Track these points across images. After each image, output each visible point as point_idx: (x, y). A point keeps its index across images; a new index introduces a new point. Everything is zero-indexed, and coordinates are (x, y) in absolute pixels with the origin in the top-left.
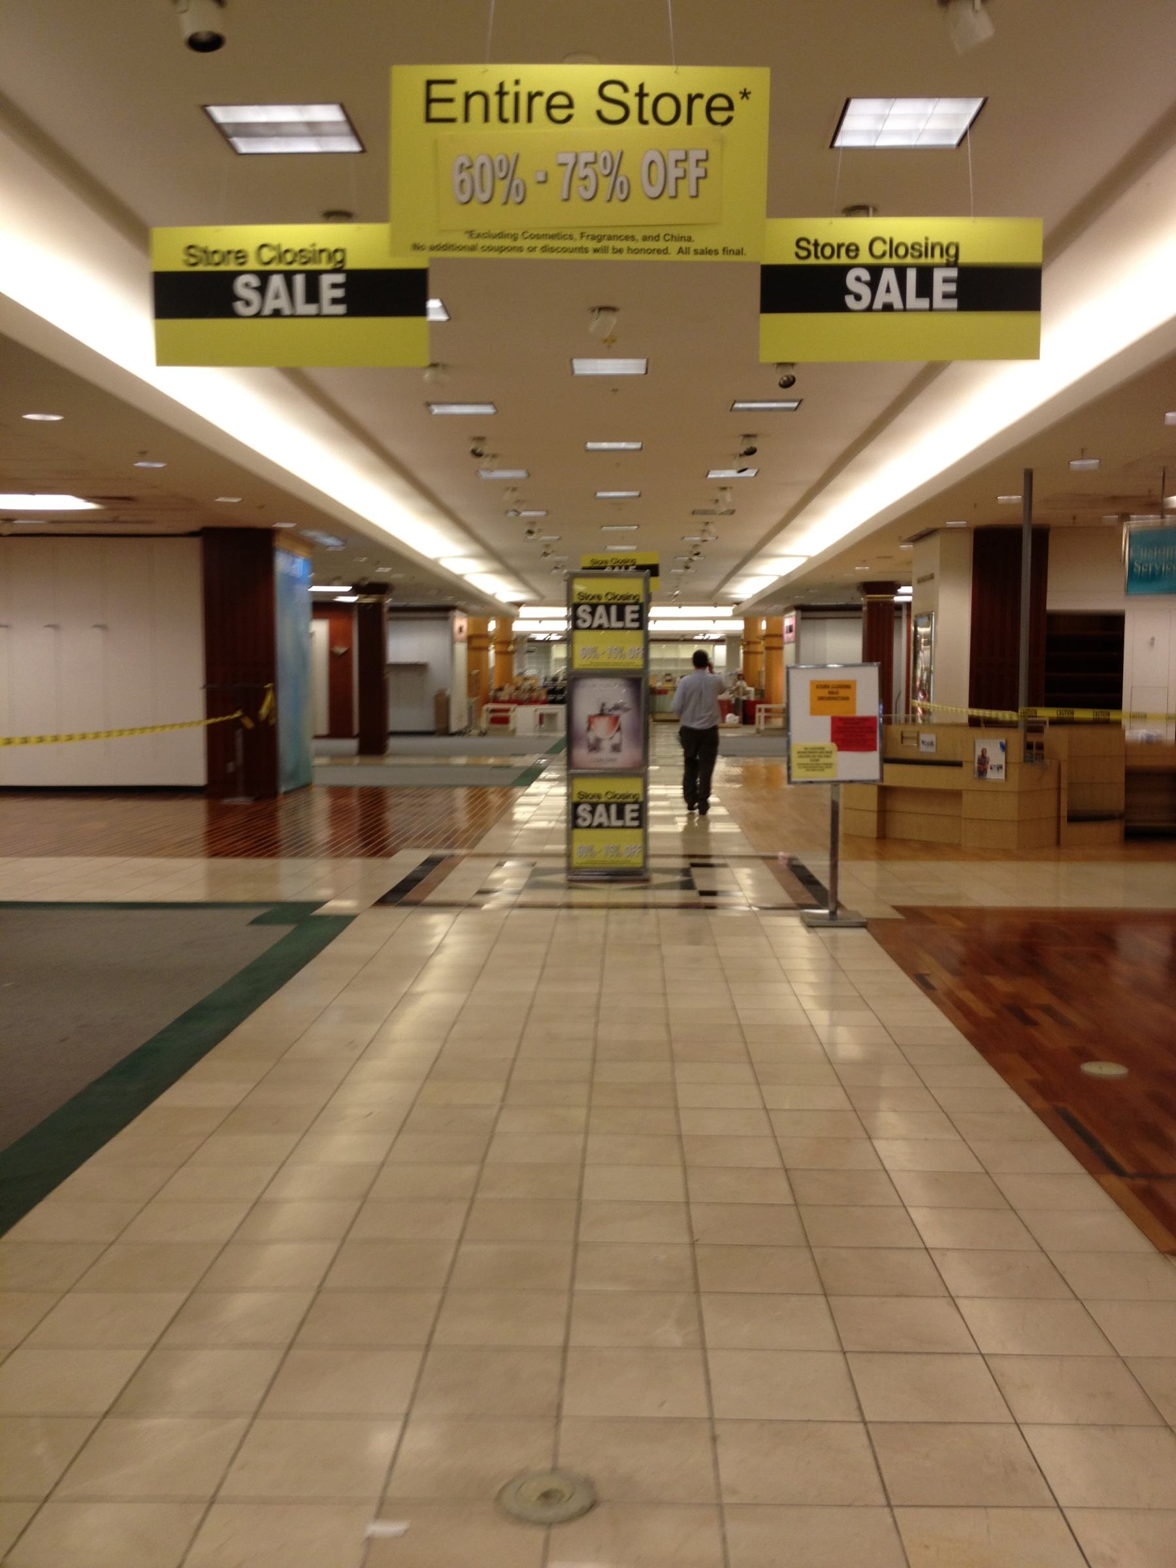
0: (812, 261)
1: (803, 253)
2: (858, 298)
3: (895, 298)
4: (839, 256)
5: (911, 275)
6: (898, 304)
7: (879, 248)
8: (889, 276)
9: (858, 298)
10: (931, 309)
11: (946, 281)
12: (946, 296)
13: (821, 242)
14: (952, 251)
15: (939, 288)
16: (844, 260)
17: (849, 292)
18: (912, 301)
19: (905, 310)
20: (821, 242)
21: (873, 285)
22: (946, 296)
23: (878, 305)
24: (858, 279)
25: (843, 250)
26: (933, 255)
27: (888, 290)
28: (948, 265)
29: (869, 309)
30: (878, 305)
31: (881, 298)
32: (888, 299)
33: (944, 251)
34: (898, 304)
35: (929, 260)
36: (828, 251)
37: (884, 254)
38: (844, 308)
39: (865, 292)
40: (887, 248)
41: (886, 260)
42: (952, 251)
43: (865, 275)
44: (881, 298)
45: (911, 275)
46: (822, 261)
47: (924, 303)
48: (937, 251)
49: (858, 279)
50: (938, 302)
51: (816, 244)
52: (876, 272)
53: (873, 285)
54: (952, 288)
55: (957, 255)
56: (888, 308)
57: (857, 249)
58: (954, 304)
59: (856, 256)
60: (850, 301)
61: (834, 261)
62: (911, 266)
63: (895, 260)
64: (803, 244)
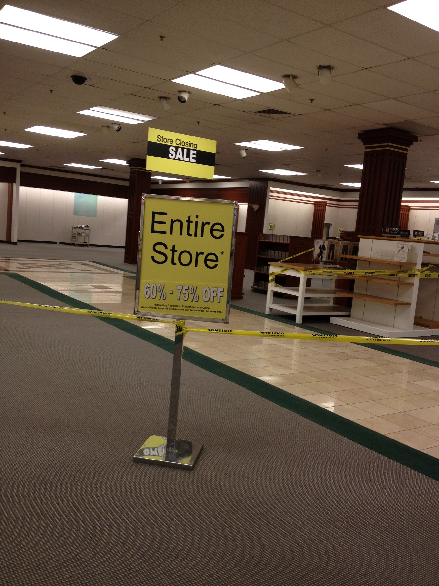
0: (161, 142)
1: (159, 140)
2: (172, 155)
6: (182, 159)
7: (178, 142)
8: (180, 150)
9: (172, 155)
10: (189, 162)
11: (194, 154)
12: (193, 158)
13: (164, 137)
14: (195, 146)
15: (192, 156)
16: (169, 144)
17: (170, 153)
20: (164, 137)
21: (176, 152)
22: (193, 158)
23: (177, 158)
24: (172, 150)
25: (169, 141)
28: (194, 150)
29: (174, 159)
30: (177, 158)
36: (165, 140)
39: (174, 153)
40: (180, 142)
41: (179, 146)
43: (174, 149)
45: (185, 151)
46: (164, 143)
47: (188, 159)
49: (172, 150)
51: (162, 138)
52: (177, 148)
53: (176, 152)
54: (195, 156)
55: (196, 148)
56: (179, 159)
58: (195, 161)
60: (170, 155)
61: (167, 143)
62: (186, 148)
63: (182, 146)
64: (159, 137)
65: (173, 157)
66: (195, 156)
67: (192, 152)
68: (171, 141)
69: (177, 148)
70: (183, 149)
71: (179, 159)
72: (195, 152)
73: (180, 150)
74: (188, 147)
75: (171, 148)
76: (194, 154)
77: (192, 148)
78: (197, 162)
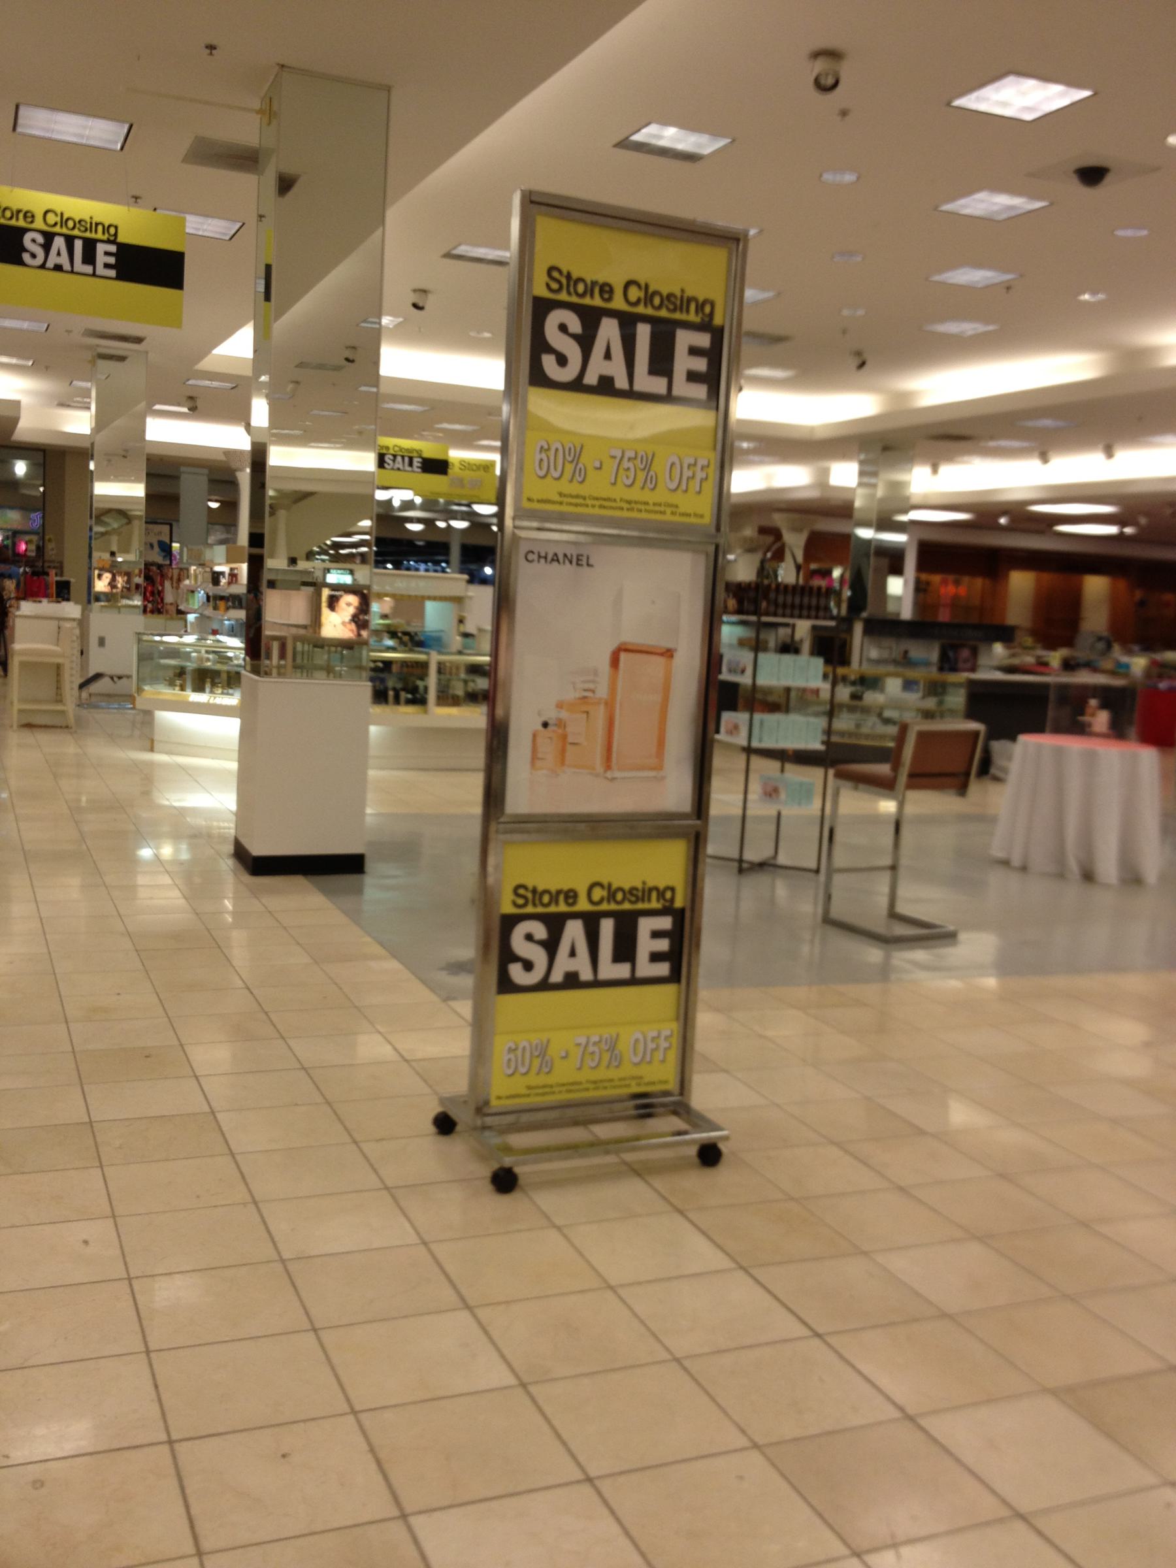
2: (34, 256)
3: (64, 260)
4: (17, 219)
5: (78, 244)
6: (67, 267)
7: (51, 218)
8: (59, 242)
9: (34, 256)
10: (94, 275)
11: (107, 253)
12: (107, 266)
14: (112, 231)
15: (101, 259)
16: (21, 223)
18: (79, 265)
19: (72, 272)
21: (47, 247)
22: (107, 266)
23: (50, 264)
24: (34, 241)
26: (96, 231)
27: (59, 254)
28: (109, 242)
30: (50, 264)
31: (52, 260)
32: (59, 261)
33: (106, 229)
34: (67, 267)
35: (93, 236)
37: (56, 224)
38: (21, 263)
39: (40, 252)
40: (58, 219)
41: (57, 229)
42: (112, 231)
43: (40, 239)
44: (52, 260)
45: (78, 244)
47: (89, 269)
48: (100, 228)
50: (100, 270)
52: (49, 237)
53: (47, 247)
54: (112, 260)
55: (116, 235)
56: (58, 268)
57: (33, 216)
59: (32, 222)
60: (26, 257)
61: (13, 222)
63: (64, 231)
65: (39, 260)
66: (112, 260)
67: (101, 248)
68: (29, 216)
69: (49, 237)
70: (70, 241)
71: (58, 268)
72: (113, 248)
73: (59, 242)
74: (88, 235)
75: (28, 238)
76: (107, 253)
77: (99, 236)
78: (119, 277)
